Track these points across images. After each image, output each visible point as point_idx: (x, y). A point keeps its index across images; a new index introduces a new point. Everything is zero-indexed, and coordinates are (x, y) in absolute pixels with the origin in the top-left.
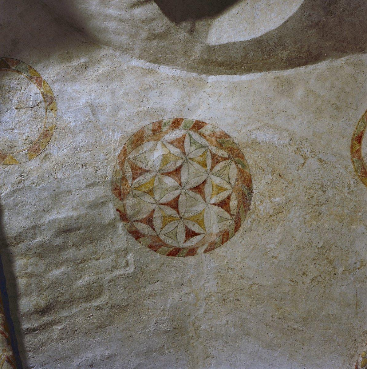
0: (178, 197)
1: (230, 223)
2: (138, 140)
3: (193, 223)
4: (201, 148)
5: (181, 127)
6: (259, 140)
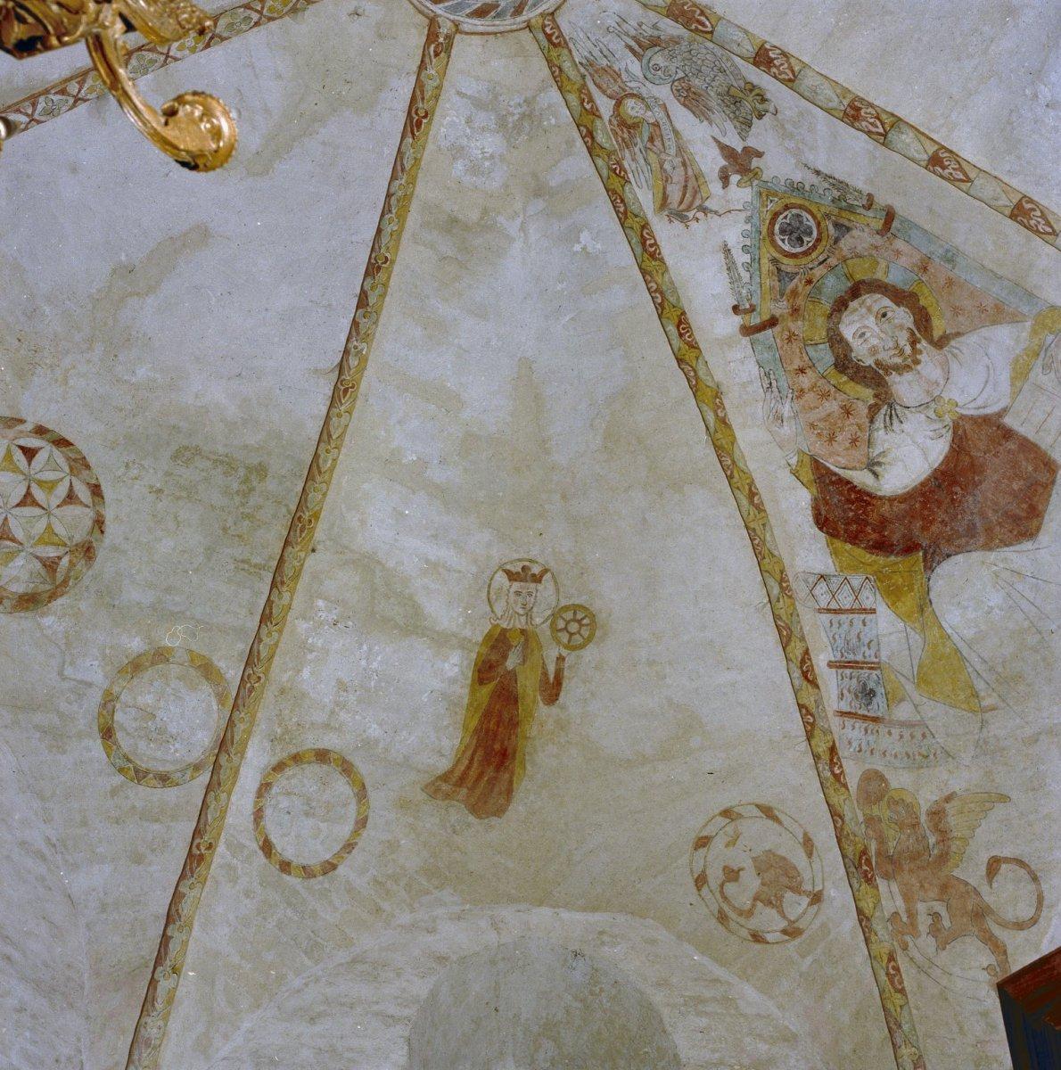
0: (18, 505)
2: (28, 601)
3: (18, 463)
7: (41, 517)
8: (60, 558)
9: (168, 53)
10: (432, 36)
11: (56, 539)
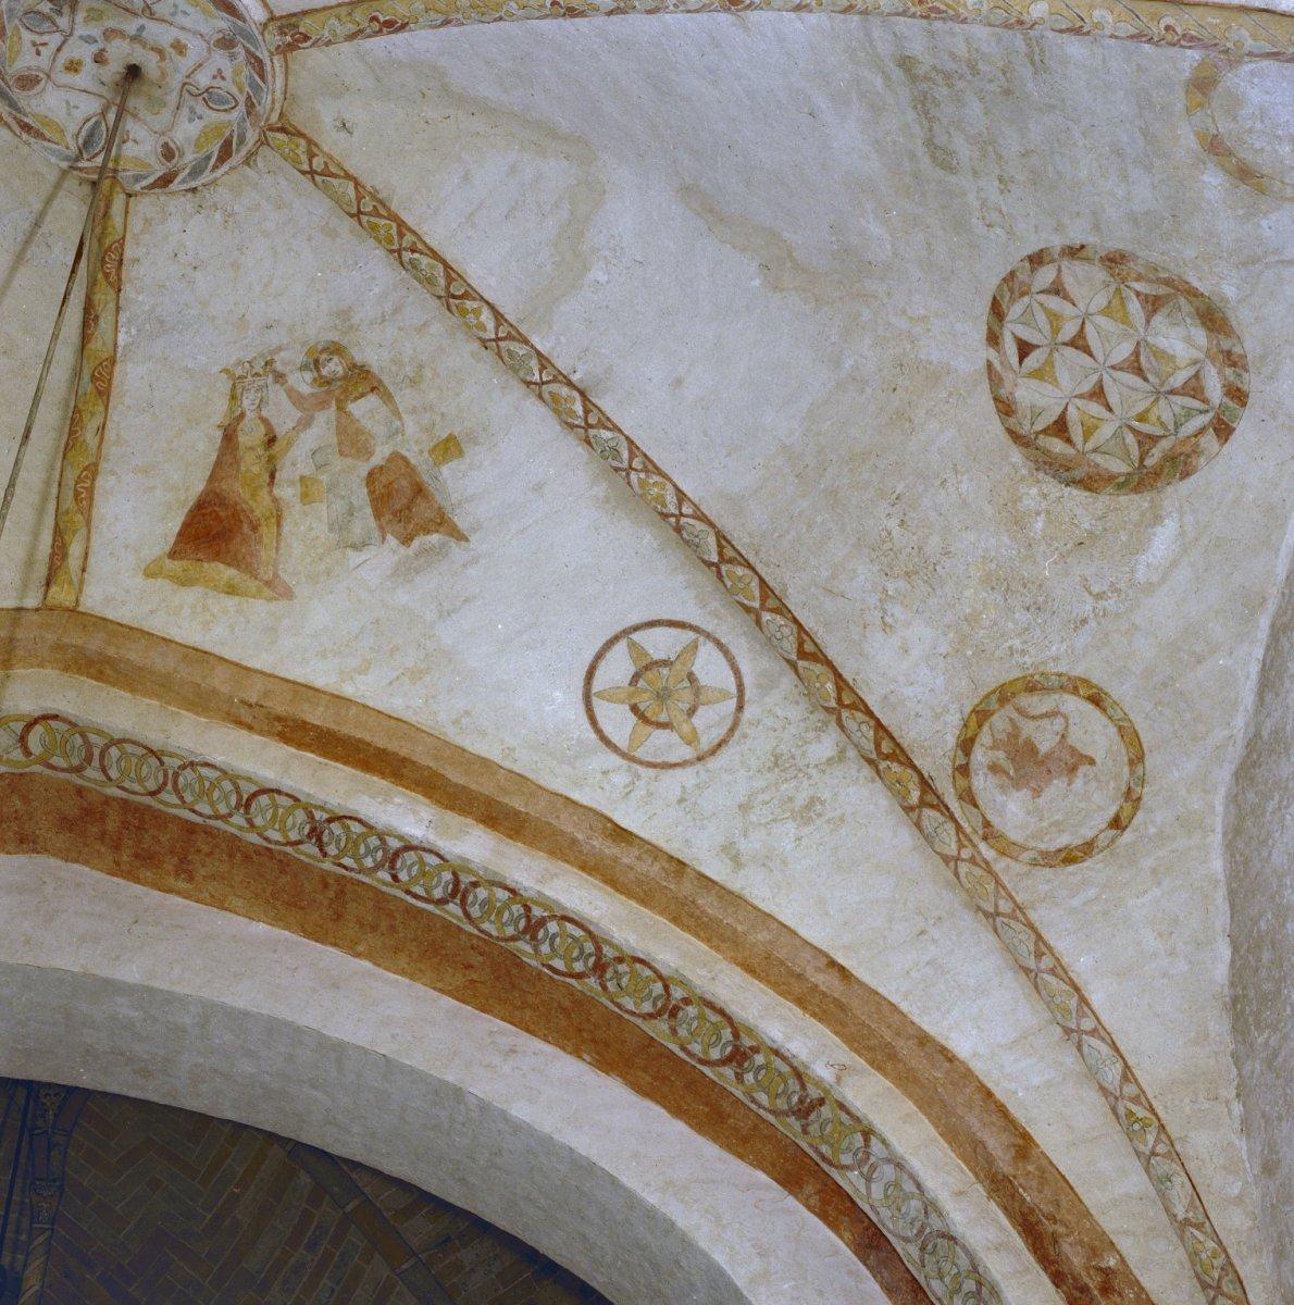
0: (1091, 355)
1: (1025, 429)
3: (1041, 362)
4: (1175, 423)
5: (1226, 400)
6: (1159, 529)
7: (1096, 327)
8: (1138, 294)
9: (493, 340)
10: (291, 47)
11: (1116, 302)
